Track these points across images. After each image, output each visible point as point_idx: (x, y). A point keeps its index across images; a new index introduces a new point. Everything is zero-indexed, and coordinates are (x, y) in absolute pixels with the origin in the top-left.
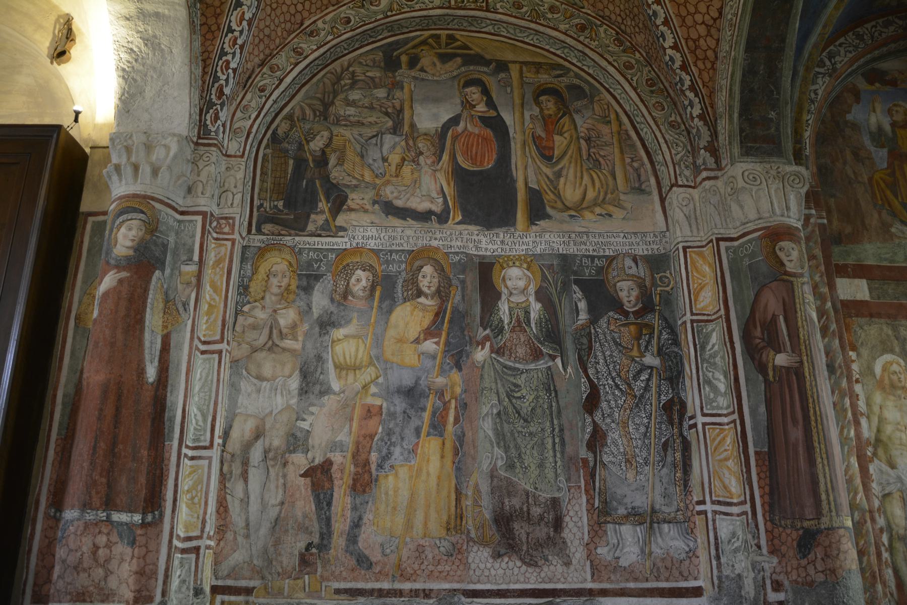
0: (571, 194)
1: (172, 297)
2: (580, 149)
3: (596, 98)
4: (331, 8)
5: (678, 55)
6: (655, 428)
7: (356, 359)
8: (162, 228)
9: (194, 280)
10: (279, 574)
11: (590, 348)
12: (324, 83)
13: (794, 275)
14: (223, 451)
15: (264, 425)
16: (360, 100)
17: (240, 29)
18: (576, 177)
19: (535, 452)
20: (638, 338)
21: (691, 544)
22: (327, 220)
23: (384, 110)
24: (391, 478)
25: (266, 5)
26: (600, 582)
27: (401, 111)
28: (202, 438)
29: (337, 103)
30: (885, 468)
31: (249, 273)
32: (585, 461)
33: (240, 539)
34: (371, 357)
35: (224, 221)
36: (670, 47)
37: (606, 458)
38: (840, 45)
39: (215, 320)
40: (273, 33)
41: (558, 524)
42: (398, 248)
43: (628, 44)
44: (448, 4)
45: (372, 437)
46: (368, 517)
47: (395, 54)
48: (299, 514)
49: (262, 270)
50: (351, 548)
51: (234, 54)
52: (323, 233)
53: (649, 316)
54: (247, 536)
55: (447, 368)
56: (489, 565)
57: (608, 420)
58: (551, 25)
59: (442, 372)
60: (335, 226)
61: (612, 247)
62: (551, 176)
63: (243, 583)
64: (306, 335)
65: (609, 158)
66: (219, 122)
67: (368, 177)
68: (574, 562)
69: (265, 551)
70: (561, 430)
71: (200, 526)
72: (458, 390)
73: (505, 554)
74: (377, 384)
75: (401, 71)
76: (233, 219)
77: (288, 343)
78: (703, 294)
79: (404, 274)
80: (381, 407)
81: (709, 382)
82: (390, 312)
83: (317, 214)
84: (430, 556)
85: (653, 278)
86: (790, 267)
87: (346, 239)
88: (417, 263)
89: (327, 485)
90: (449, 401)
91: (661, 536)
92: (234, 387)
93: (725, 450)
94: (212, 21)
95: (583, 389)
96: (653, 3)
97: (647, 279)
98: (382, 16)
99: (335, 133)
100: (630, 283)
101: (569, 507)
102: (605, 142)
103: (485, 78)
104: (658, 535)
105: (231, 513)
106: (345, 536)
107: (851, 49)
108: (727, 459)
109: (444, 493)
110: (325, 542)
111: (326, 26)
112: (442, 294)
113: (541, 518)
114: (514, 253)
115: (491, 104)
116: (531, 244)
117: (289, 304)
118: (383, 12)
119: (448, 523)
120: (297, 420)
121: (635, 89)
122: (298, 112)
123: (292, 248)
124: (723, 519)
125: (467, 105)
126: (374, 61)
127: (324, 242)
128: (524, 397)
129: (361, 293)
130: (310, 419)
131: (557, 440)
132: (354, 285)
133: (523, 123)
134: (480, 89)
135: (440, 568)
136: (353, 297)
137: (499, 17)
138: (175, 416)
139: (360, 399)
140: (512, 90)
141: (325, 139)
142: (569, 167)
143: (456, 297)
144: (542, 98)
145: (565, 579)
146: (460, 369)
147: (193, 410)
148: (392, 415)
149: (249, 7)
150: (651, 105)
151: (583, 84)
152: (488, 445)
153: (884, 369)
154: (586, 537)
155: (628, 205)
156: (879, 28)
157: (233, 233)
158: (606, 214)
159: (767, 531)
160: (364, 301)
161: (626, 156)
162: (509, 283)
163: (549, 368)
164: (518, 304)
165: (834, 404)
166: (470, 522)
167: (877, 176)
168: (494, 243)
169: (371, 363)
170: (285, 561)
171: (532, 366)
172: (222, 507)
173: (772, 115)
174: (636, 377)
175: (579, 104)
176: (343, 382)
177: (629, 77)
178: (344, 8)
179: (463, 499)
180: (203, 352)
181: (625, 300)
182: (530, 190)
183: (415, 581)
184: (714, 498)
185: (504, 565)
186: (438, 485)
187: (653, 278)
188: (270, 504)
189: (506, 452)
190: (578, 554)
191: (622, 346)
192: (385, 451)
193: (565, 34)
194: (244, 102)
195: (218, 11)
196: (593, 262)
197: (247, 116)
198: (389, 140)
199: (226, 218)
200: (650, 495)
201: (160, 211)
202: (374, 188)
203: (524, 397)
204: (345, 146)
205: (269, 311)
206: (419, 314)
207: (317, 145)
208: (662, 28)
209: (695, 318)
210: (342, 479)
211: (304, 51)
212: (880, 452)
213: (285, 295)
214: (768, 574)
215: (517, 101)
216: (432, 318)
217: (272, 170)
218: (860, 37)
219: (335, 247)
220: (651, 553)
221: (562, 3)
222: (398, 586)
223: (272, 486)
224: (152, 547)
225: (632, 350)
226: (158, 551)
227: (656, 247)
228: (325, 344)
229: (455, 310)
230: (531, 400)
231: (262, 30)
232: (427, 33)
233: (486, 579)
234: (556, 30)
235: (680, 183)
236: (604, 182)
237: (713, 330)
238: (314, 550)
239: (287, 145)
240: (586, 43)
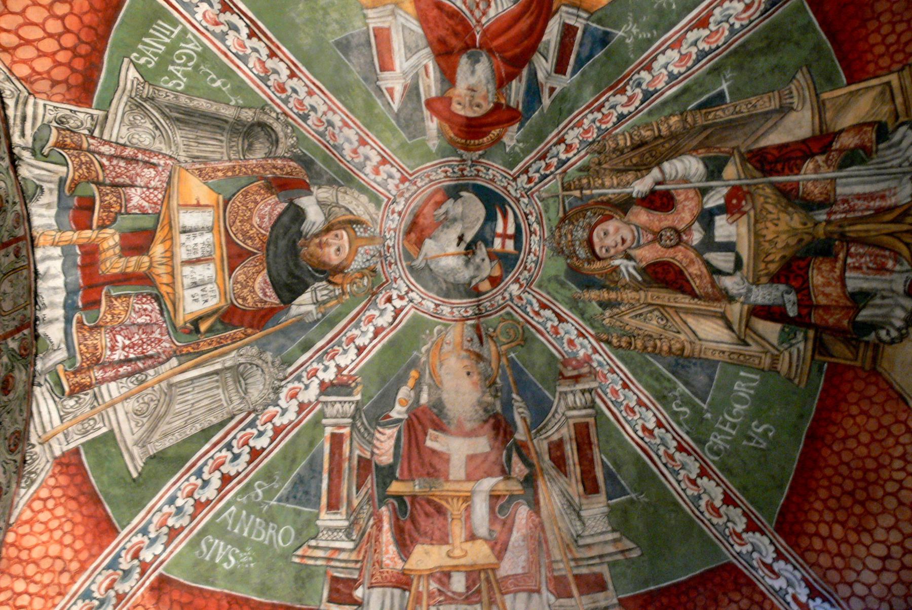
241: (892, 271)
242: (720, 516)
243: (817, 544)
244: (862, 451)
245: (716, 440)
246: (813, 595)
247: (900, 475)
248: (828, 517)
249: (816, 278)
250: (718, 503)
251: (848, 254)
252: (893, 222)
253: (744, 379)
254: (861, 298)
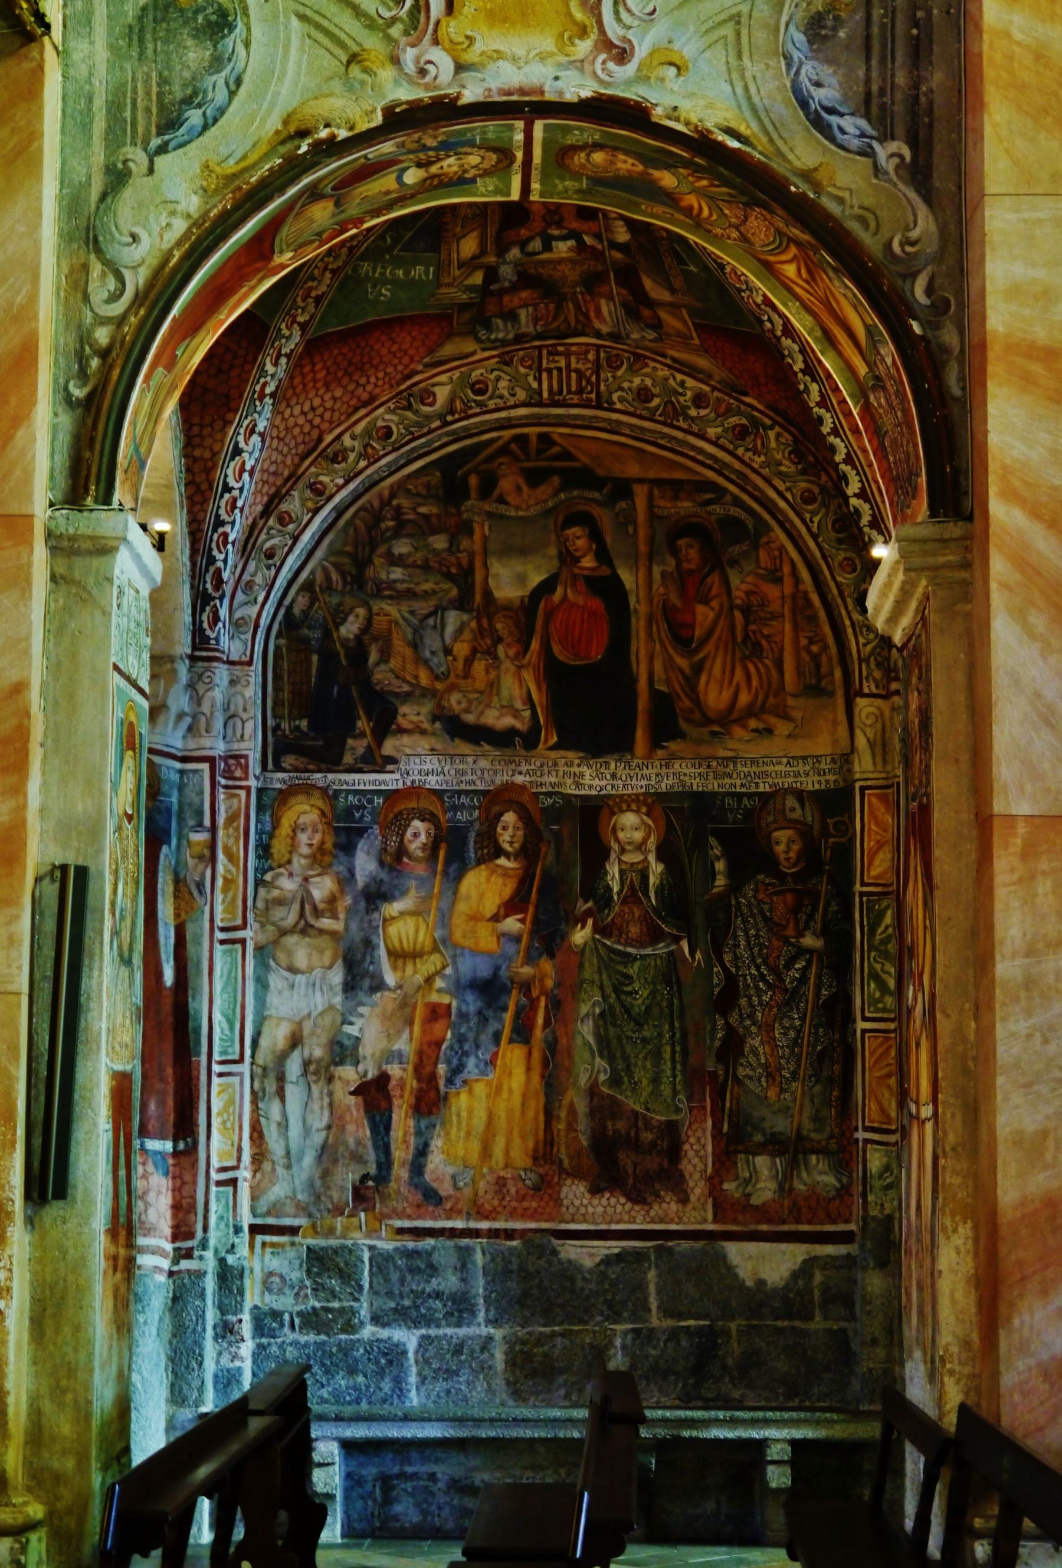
0: (715, 698)
1: (182, 876)
2: (732, 626)
3: (764, 540)
4: (362, 412)
5: (867, 506)
6: (810, 1032)
7: (415, 943)
8: (165, 788)
9: (207, 852)
10: (329, 1211)
11: (728, 923)
12: (356, 529)
14: (252, 1064)
15: (301, 1030)
16: (409, 555)
17: (239, 485)
18: (724, 672)
19: (648, 1064)
20: (795, 910)
21: (845, 1180)
22: (369, 748)
23: (444, 569)
24: (464, 1097)
25: (272, 438)
26: (725, 1223)
27: (470, 571)
28: (230, 1050)
29: (377, 561)
31: (268, 827)
32: (714, 1075)
33: (280, 1170)
34: (435, 941)
35: (232, 761)
36: (855, 495)
37: (741, 1072)
39: (234, 900)
40: (281, 466)
41: (675, 1153)
42: (469, 788)
43: (811, 459)
44: (536, 397)
45: (438, 1044)
46: (437, 1144)
47: (460, 473)
48: (351, 1141)
49: (286, 823)
50: (416, 1180)
51: (233, 523)
52: (366, 768)
54: (288, 1167)
55: (534, 953)
56: (585, 1201)
57: (748, 1022)
58: (695, 428)
59: (529, 960)
60: (382, 757)
61: (770, 780)
62: (687, 671)
63: (287, 1221)
64: (349, 911)
65: (776, 639)
66: (220, 625)
67: (424, 679)
68: (693, 1198)
69: (311, 1184)
70: (684, 1035)
71: (235, 1154)
72: (550, 983)
73: (605, 1189)
74: (444, 977)
75: (469, 503)
76: (246, 757)
77: (326, 923)
78: (881, 855)
79: (477, 826)
80: (449, 1006)
81: (875, 976)
82: (459, 878)
83: (355, 737)
84: (513, 1190)
85: (824, 825)
87: (397, 776)
88: (496, 809)
89: (384, 1104)
90: (538, 999)
91: (806, 1169)
92: (262, 984)
93: (889, 1065)
94: (201, 478)
95: (716, 981)
96: (829, 434)
97: (816, 826)
98: (437, 423)
99: (375, 609)
100: (789, 832)
101: (690, 1133)
102: (771, 613)
103: (596, 511)
104: (802, 1167)
105: (267, 1139)
106: (407, 1167)
108: (888, 1076)
109: (530, 1114)
110: (384, 1173)
111: (356, 444)
112: (527, 852)
113: (653, 1144)
114: (630, 791)
115: (603, 555)
116: (653, 777)
117: (325, 869)
118: (441, 416)
119: (535, 1150)
120: (343, 1023)
121: (815, 537)
122: (319, 577)
123: (324, 790)
124: (876, 1150)
125: (568, 558)
126: (428, 486)
127: (366, 781)
128: (637, 992)
129: (419, 853)
130: (359, 1022)
131: (678, 1049)
132: (410, 842)
133: (650, 586)
134: (587, 531)
135: (525, 1204)
136: (410, 858)
137: (615, 416)
138: (200, 1027)
139: (423, 996)
140: (636, 531)
141: (361, 619)
142: (715, 656)
143: (548, 857)
144: (682, 542)
145: (680, 1218)
146: (552, 956)
147: (217, 1016)
148: (463, 1016)
149: (251, 454)
150: (836, 564)
151: (744, 516)
152: (587, 1055)
154: (709, 1170)
155: (798, 715)
157: (246, 778)
158: (765, 729)
160: (423, 865)
161: (802, 634)
162: (621, 835)
163: (671, 954)
164: (632, 864)
166: (563, 1150)
168: (600, 776)
169: (435, 949)
170: (336, 1195)
171: (648, 951)
172: (257, 1134)
174: (789, 965)
175: (736, 549)
176: (399, 974)
177: (808, 516)
178: (381, 410)
179: (554, 1123)
180: (223, 942)
181: (782, 856)
182: (655, 694)
183: (494, 1219)
184: (867, 1124)
185: (604, 1202)
186: (523, 1104)
188: (314, 1129)
189: (610, 1064)
190: (697, 1189)
191: (776, 924)
192: (455, 1061)
193: (715, 444)
194: (246, 577)
195: (210, 464)
196: (740, 802)
197: (252, 597)
198: (453, 619)
199: (237, 757)
200: (796, 1118)
201: (160, 766)
202: (434, 696)
203: (637, 992)
204: (390, 631)
205: (298, 879)
206: (497, 881)
207: (350, 629)
208: (842, 467)
209: (865, 889)
210: (402, 1097)
211: (325, 487)
213: (319, 858)
215: (643, 548)
216: (515, 885)
217: (290, 672)
219: (383, 787)
220: (792, 1189)
221: (714, 389)
222: (473, 1225)
223: (316, 1106)
224: (187, 1177)
225: (786, 927)
226: (195, 1182)
227: (832, 778)
228: (374, 924)
229: (545, 873)
230: (645, 995)
231: (267, 471)
232: (507, 434)
233: (581, 1218)
234: (702, 437)
235: (866, 690)
236: (764, 676)
237: (888, 907)
238: (371, 1183)
239: (306, 631)
240: (746, 459)
241: (535, 326)
242: (303, 301)
243: (307, 369)
244: (384, 351)
245: (366, 267)
246: (273, 395)
247: (373, 380)
248: (329, 363)
249: (524, 294)
250: (314, 294)
251: (546, 304)
252: (577, 320)
253: (427, 272)
254: (512, 316)
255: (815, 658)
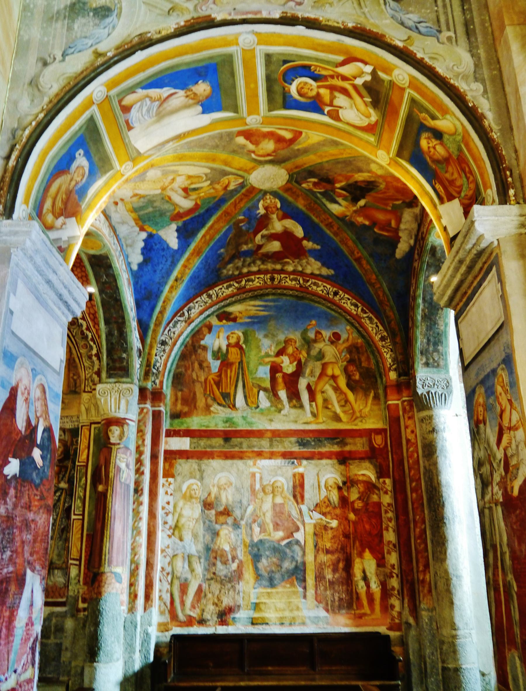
13: (114, 444)
30: (177, 541)
36: (81, 319)
38: (197, 302)
53: (67, 462)
85: (72, 441)
86: (112, 440)
107: (202, 304)
153: (188, 488)
156: (223, 289)
159: (84, 573)
165: (133, 510)
167: (210, 378)
173: (124, 355)
187: (72, 441)
212: (176, 532)
214: (80, 594)
218: (210, 296)
255: (75, 381)
